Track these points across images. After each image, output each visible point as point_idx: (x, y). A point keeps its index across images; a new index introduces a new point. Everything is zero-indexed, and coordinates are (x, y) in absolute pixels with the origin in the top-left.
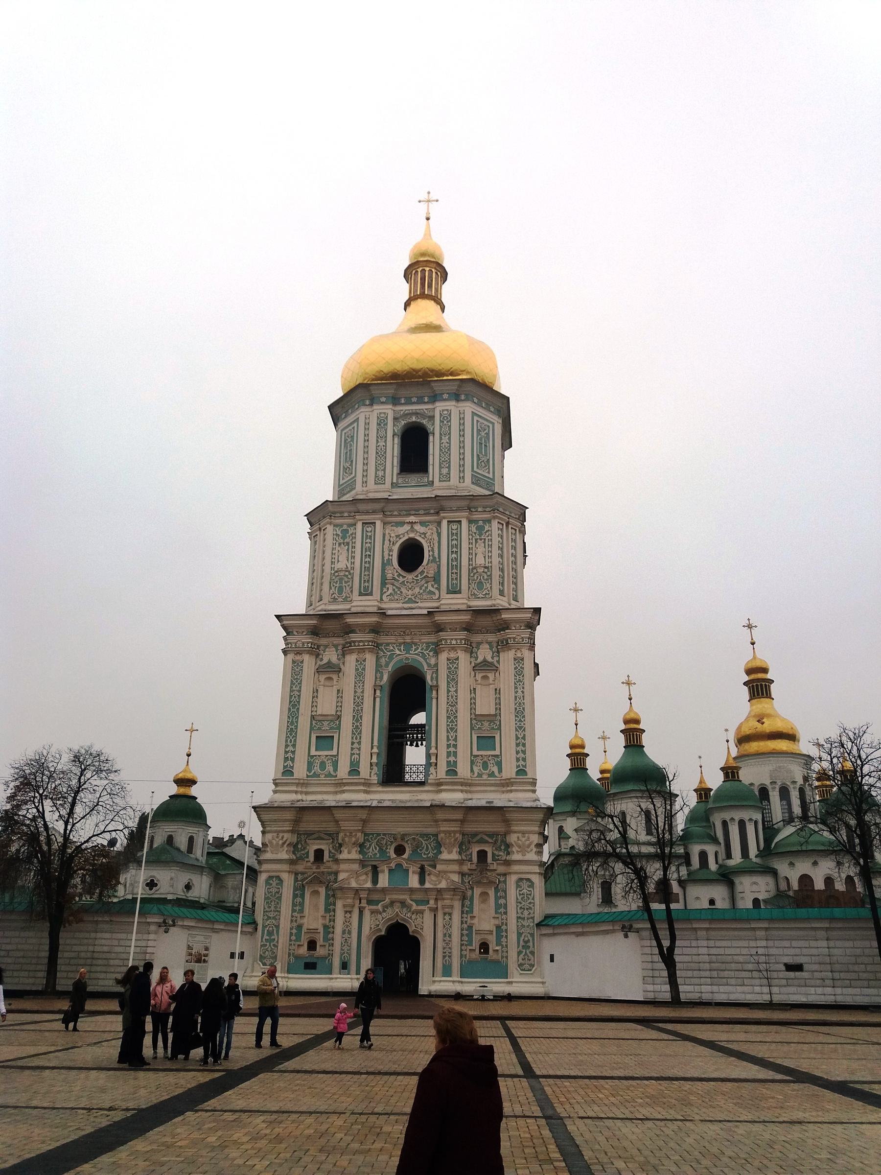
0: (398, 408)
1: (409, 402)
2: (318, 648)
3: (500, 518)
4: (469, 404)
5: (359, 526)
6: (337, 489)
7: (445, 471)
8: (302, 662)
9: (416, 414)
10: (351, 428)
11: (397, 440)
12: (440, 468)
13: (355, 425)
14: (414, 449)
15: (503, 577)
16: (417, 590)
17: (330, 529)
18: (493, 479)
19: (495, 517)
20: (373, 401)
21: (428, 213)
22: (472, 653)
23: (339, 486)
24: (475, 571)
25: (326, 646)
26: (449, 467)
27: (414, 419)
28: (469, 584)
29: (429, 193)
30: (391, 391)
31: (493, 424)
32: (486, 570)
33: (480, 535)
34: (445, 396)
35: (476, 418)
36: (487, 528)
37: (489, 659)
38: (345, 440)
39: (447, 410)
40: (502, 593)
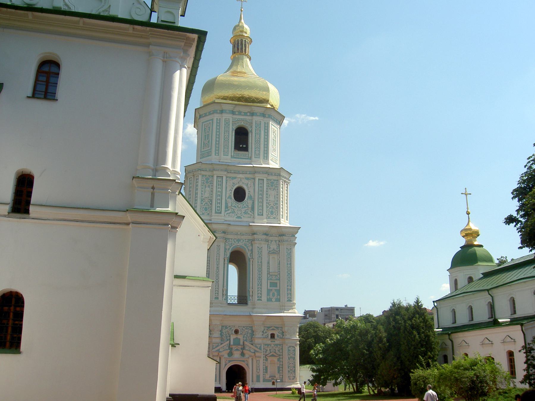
0: (235, 116)
1: (240, 113)
3: (282, 180)
5: (215, 178)
6: (200, 153)
9: (242, 120)
10: (209, 122)
11: (234, 134)
12: (255, 150)
13: (211, 122)
14: (242, 138)
17: (200, 177)
20: (222, 112)
23: (201, 152)
26: (259, 151)
27: (242, 123)
30: (231, 108)
34: (258, 114)
38: (205, 129)
40: (282, 218)
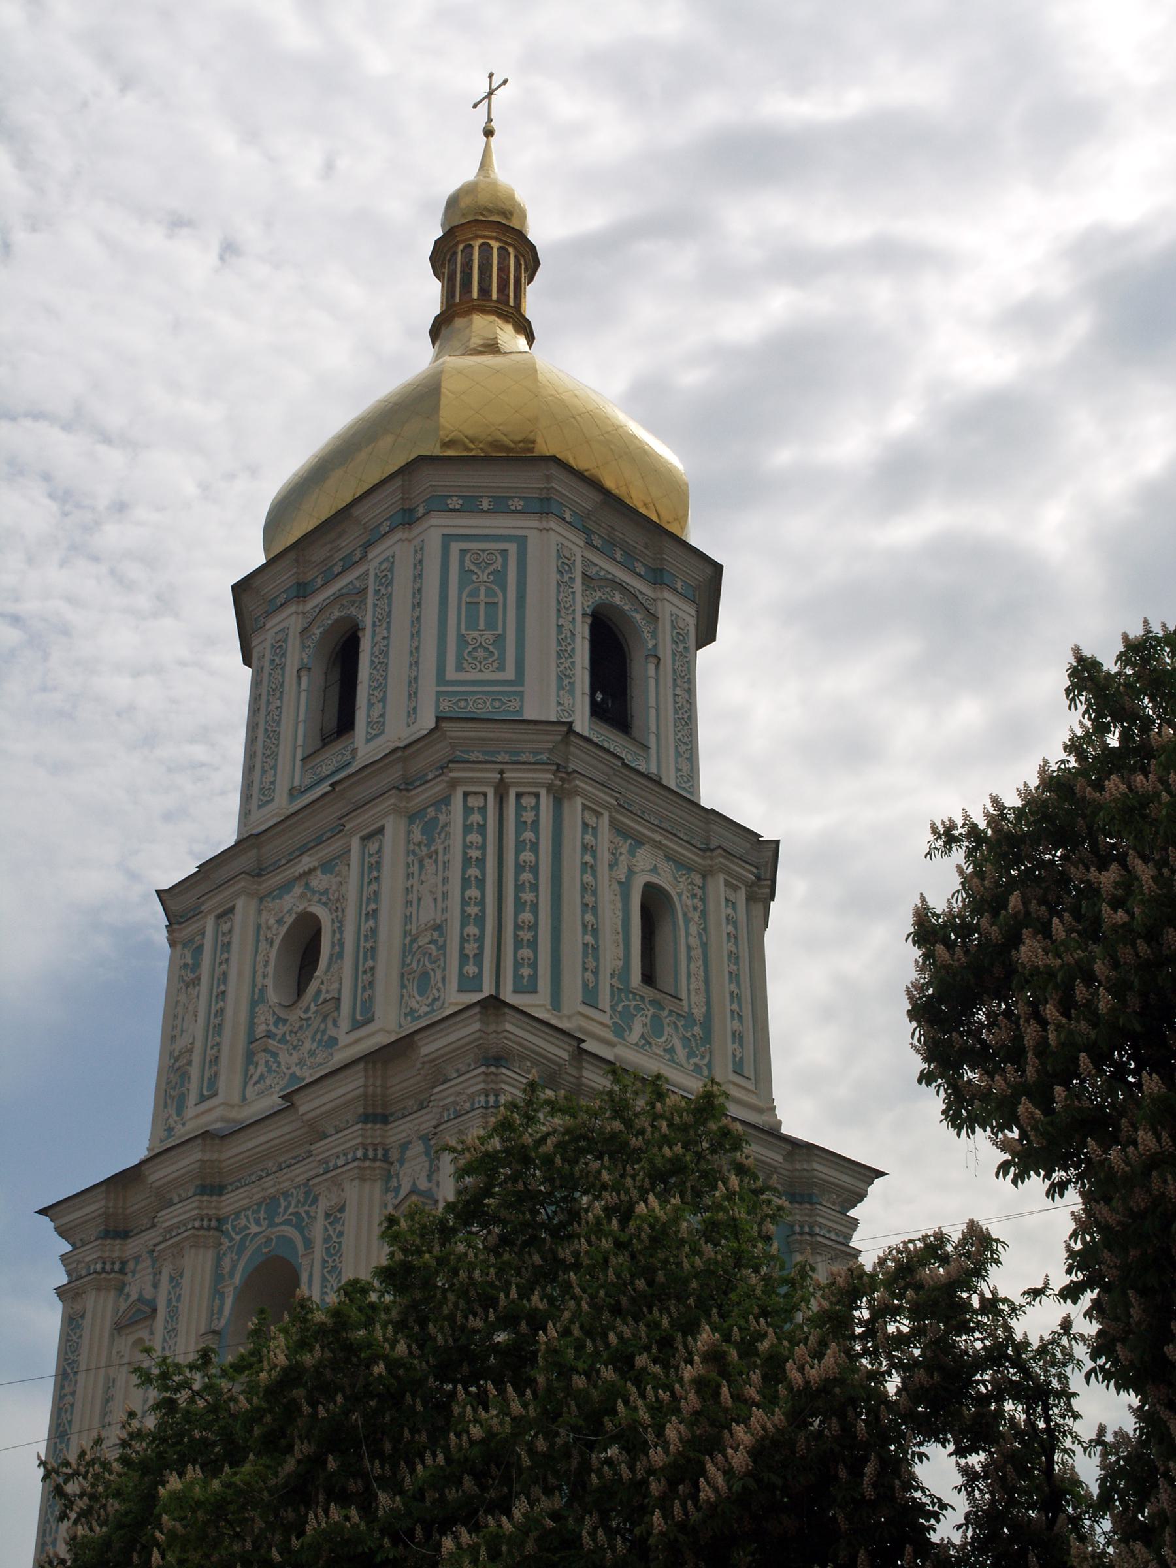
2: (122, 1271)
4: (435, 520)
7: (376, 711)
8: (82, 1317)
15: (480, 940)
16: (308, 1045)
18: (520, 679)
19: (453, 784)
21: (490, 120)
22: (388, 1177)
24: (415, 946)
25: (137, 1259)
27: (337, 614)
28: (403, 986)
29: (491, 76)
31: (522, 541)
32: (436, 934)
33: (431, 841)
35: (455, 547)
36: (442, 818)
37: (423, 1185)
39: (387, 559)
